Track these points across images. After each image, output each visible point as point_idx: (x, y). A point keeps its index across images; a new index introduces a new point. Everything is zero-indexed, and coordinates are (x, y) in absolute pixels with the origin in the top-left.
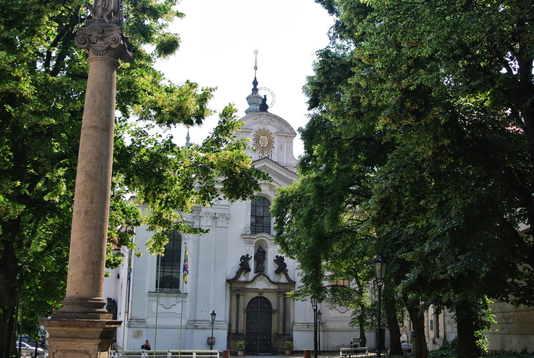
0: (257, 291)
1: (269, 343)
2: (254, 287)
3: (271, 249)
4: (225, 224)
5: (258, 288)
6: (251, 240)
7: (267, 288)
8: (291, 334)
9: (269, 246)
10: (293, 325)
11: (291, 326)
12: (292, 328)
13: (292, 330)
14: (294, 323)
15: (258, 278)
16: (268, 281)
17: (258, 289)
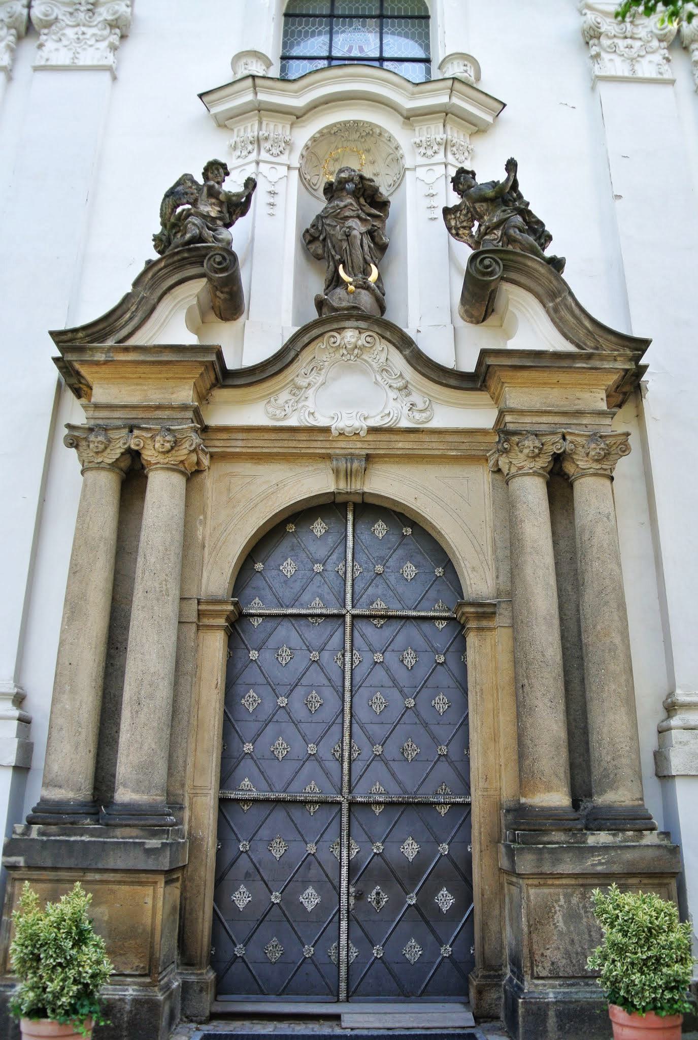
0: (319, 447)
1: (445, 900)
2: (293, 422)
3: (421, 172)
4: (88, 57)
5: (321, 421)
6: (275, 128)
7: (404, 424)
8: (654, 808)
9: (408, 162)
10: (663, 731)
11: (648, 741)
12: (660, 757)
13: (664, 777)
14: (671, 708)
15: (320, 351)
16: (409, 373)
17: (326, 430)
